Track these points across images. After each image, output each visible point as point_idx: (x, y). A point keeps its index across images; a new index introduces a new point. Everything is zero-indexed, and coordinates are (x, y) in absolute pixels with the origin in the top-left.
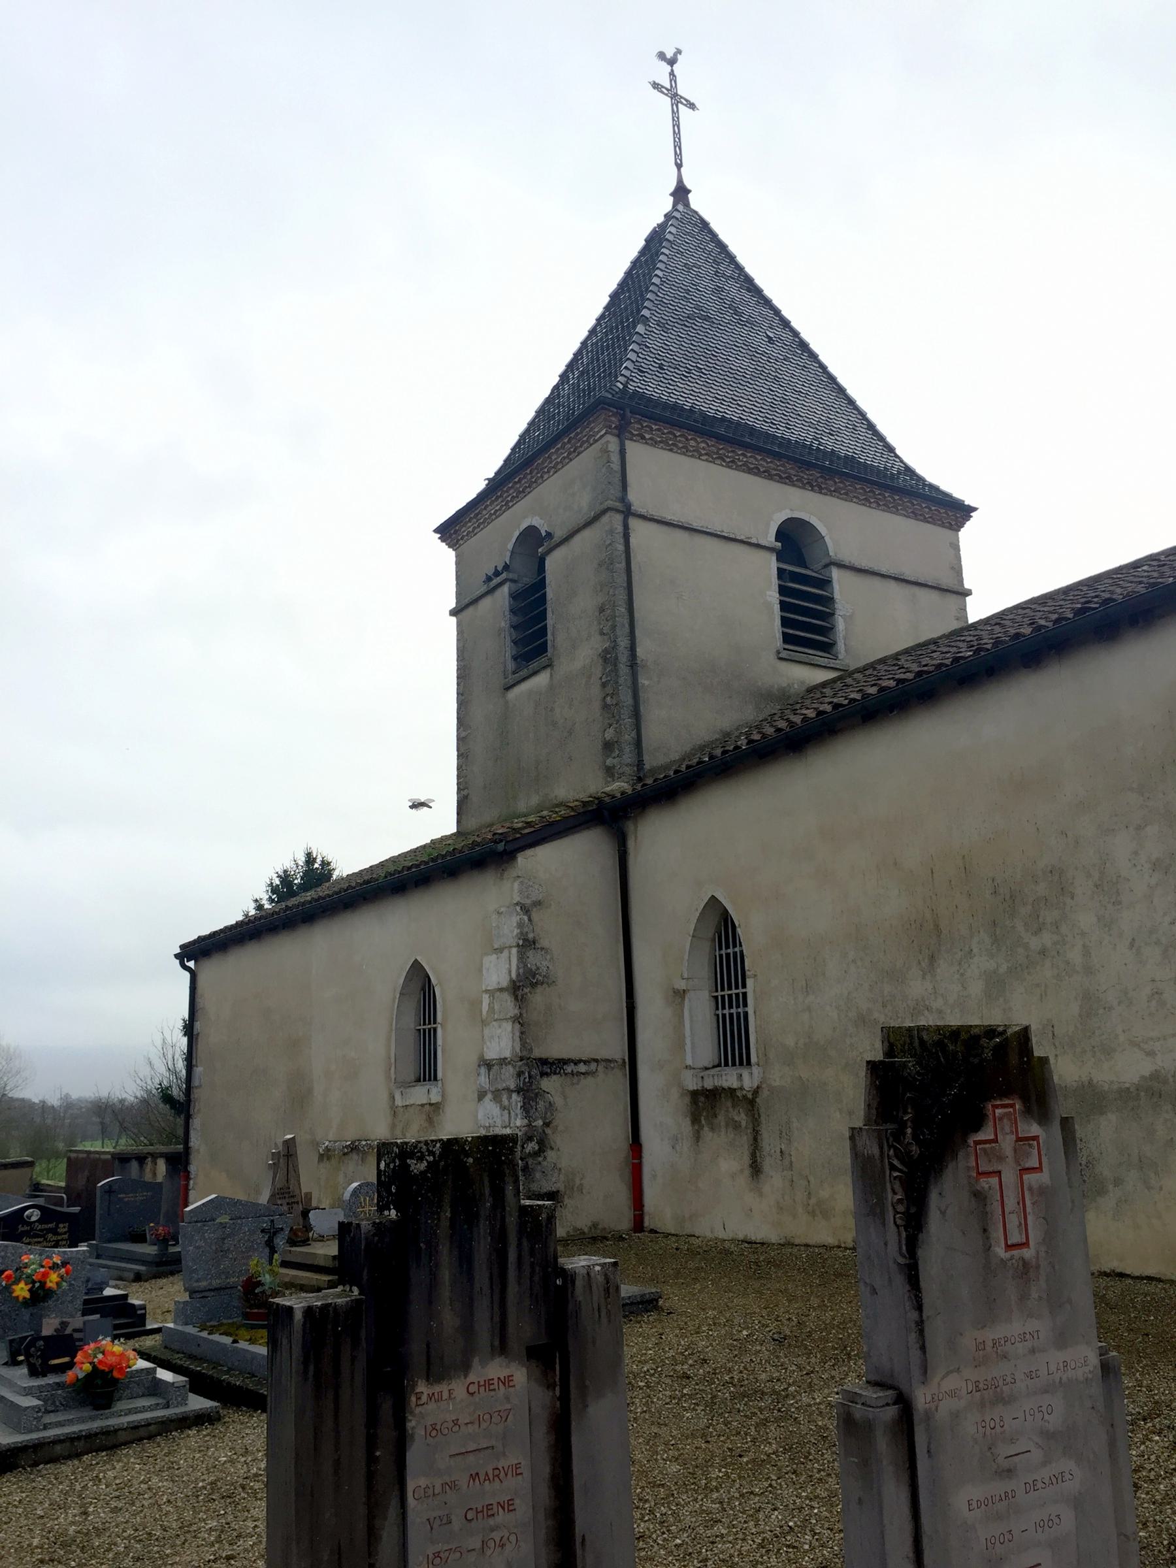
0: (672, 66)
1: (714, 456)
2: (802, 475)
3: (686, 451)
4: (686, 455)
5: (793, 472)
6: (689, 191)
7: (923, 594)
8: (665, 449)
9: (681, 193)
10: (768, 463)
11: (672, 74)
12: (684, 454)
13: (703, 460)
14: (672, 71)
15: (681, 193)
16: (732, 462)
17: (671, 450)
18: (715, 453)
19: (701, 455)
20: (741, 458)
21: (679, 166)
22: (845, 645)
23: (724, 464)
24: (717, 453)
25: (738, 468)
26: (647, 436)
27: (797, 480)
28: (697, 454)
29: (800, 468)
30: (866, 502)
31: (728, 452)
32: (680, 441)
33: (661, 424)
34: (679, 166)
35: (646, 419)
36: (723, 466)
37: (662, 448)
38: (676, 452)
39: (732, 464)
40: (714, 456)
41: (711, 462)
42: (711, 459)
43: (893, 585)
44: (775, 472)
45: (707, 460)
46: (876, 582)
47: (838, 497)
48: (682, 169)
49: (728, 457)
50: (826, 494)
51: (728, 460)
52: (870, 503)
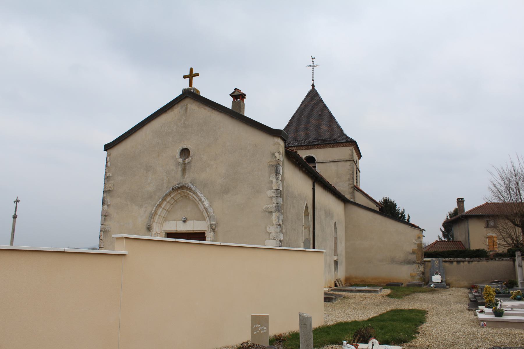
11: (313, 61)
21: (313, 80)
30: (325, 147)
34: (313, 80)
43: (332, 163)
46: (328, 164)
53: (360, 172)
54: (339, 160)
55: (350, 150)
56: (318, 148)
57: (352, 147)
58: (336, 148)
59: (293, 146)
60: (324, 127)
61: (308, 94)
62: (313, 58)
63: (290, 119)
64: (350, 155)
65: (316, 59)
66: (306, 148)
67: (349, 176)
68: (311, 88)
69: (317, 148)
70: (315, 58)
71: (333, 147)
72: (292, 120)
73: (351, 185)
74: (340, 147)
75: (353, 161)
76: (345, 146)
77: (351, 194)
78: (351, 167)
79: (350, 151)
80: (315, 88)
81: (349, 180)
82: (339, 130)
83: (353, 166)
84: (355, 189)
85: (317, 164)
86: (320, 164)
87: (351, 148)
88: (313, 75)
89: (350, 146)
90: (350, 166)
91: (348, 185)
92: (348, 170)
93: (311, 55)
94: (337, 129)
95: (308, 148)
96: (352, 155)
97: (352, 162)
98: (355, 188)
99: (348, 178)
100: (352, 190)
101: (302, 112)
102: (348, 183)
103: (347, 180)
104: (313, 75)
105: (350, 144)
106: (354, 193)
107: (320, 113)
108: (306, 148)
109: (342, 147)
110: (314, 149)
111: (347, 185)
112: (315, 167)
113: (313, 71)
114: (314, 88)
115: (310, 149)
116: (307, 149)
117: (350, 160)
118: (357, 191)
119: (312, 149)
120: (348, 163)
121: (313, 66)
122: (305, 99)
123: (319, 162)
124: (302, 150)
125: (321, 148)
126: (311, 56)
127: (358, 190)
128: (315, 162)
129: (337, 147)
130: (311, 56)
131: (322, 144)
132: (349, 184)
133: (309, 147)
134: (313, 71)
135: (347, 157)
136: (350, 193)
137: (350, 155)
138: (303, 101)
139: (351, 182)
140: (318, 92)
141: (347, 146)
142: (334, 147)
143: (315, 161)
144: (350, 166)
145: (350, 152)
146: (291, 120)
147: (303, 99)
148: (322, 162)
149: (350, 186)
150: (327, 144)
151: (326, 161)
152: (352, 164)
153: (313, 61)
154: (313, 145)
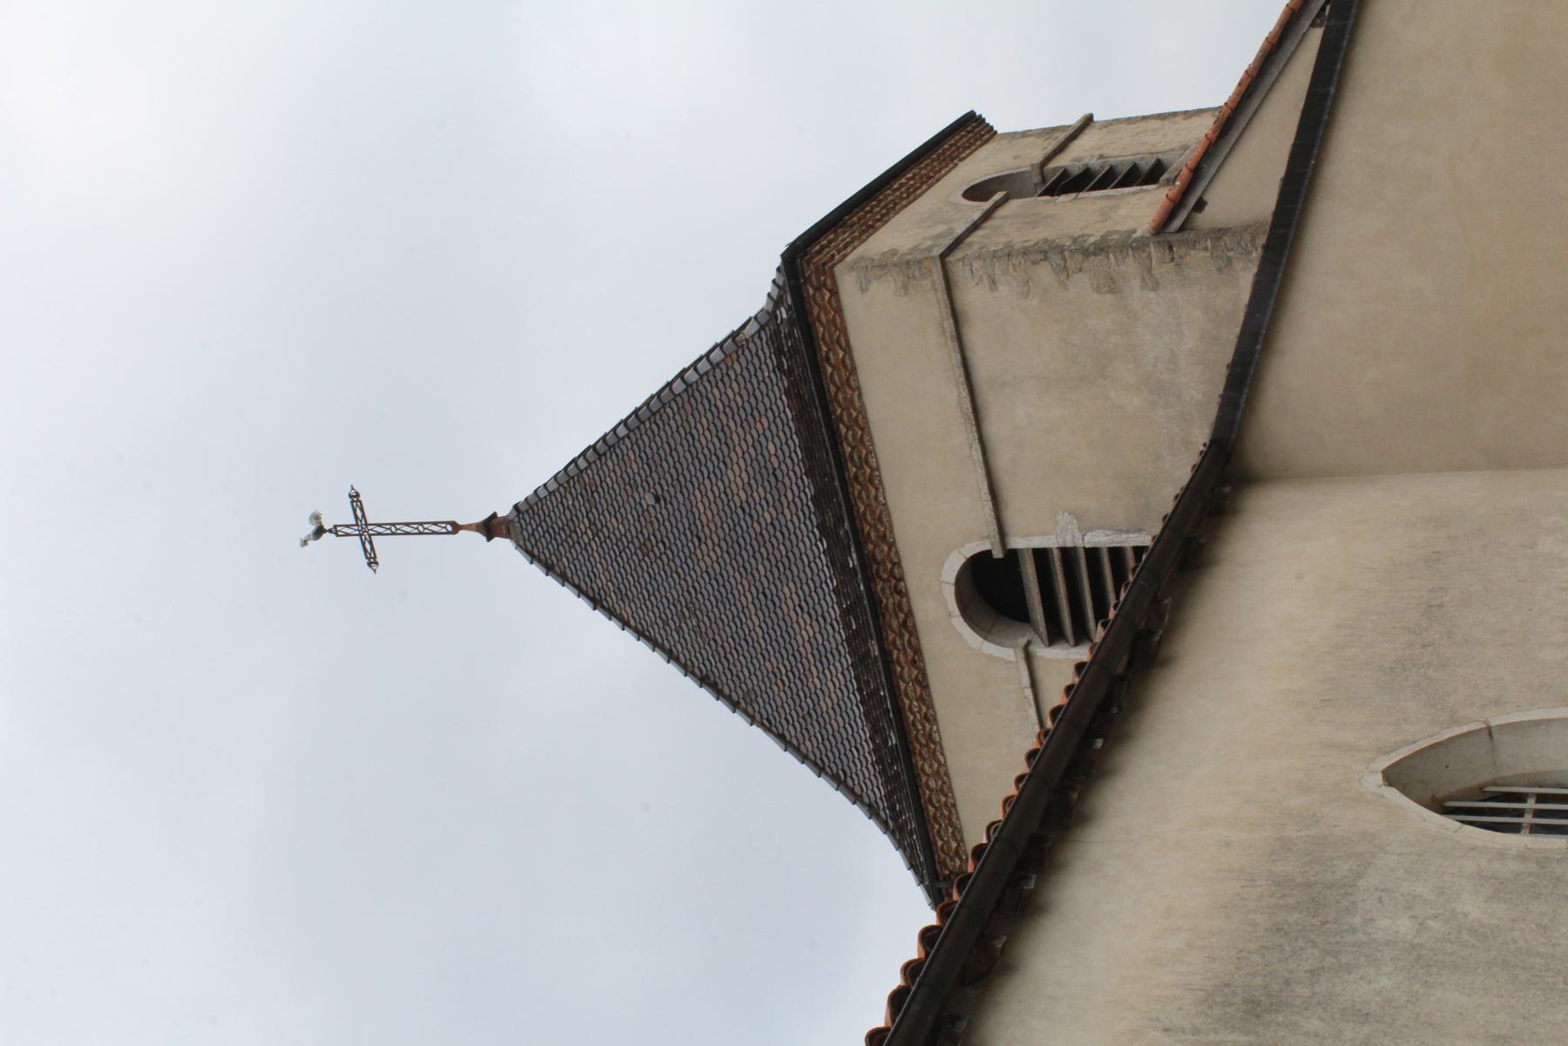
0: (325, 531)
1: (933, 746)
2: (890, 606)
3: (946, 789)
4: (950, 782)
5: (895, 624)
6: (489, 539)
7: (981, 372)
8: (957, 814)
9: (490, 528)
10: (903, 668)
11: (335, 531)
12: (950, 788)
13: (945, 759)
14: (330, 531)
15: (490, 528)
16: (928, 721)
17: (954, 805)
18: (929, 748)
19: (944, 783)
20: (916, 710)
21: (456, 528)
22: (1128, 532)
23: (935, 728)
24: (927, 745)
25: (931, 706)
26: (954, 845)
27: (902, 611)
28: (942, 774)
29: (883, 614)
31: (918, 731)
32: (939, 801)
33: (931, 835)
34: (456, 528)
35: (936, 857)
36: (938, 729)
37: (958, 818)
38: (953, 798)
39: (930, 718)
40: (933, 746)
41: (941, 747)
42: (938, 748)
43: (992, 428)
44: (909, 651)
45: (942, 754)
46: (1003, 460)
47: (892, 532)
48: (460, 522)
49: (924, 728)
50: (897, 553)
51: (927, 725)
52: (873, 470)
53: (1088, 121)
54: (959, 372)
55: (863, 290)
56: (887, 538)
57: (838, 269)
58: (867, 398)
59: (899, 709)
60: (737, 475)
61: (549, 569)
62: (312, 528)
63: (721, 707)
64: (905, 288)
65: (320, 510)
66: (904, 624)
67: (1081, 285)
68: (503, 545)
69: (892, 545)
70: (316, 517)
71: (861, 423)
72: (726, 690)
73: (1149, 270)
74: (853, 371)
75: (950, 259)
76: (844, 330)
77: (1229, 262)
78: (998, 271)
79: (875, 286)
80: (504, 511)
81: (1111, 285)
82: (736, 366)
83: (994, 255)
84: (1182, 229)
85: (1017, 542)
86: (1012, 518)
87: (847, 283)
88: (420, 529)
89: (835, 293)
90: (993, 283)
91: (1156, 286)
92: (1026, 295)
93: (298, 543)
94: (735, 385)
95: (899, 606)
96: (905, 266)
97: (959, 271)
98: (1177, 224)
99: (1098, 290)
100: (1197, 259)
101: (666, 623)
102: (1136, 293)
103: (1109, 297)
104: (420, 529)
105: (816, 289)
106: (1219, 233)
107: (650, 500)
108: (904, 624)
109: (848, 349)
110: (898, 564)
111: (1152, 295)
112: (1041, 555)
113: (393, 529)
114: (504, 518)
115: (903, 594)
116: (910, 614)
117: (941, 285)
118: (1200, 205)
119: (901, 579)
120: (973, 296)
121: (364, 530)
122: (581, 592)
123: (994, 527)
124: (918, 651)
125: (882, 517)
126: (305, 543)
127: (1192, 201)
128: (998, 554)
129: (859, 388)
130: (305, 543)
131: (851, 508)
132: (1144, 285)
133: (890, 601)
134: (393, 529)
135: (927, 306)
136: (1220, 270)
137: (905, 288)
138: (597, 602)
139: (1130, 266)
140: (520, 498)
141: (839, 310)
142: (862, 411)
143: (987, 554)
144: (993, 283)
145: (884, 290)
146: (735, 706)
147: (582, 604)
148: (989, 506)
149: (1162, 269)
150: (841, 468)
151: (981, 472)
152: (977, 265)
153: (335, 531)
154: (868, 581)
